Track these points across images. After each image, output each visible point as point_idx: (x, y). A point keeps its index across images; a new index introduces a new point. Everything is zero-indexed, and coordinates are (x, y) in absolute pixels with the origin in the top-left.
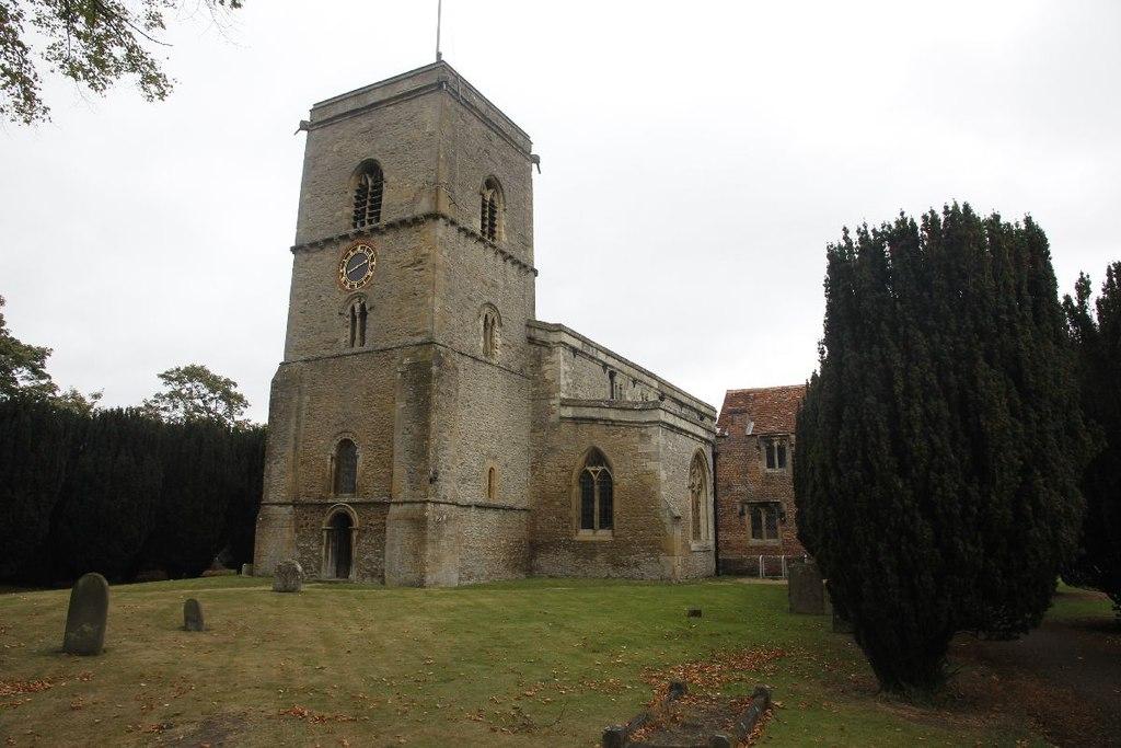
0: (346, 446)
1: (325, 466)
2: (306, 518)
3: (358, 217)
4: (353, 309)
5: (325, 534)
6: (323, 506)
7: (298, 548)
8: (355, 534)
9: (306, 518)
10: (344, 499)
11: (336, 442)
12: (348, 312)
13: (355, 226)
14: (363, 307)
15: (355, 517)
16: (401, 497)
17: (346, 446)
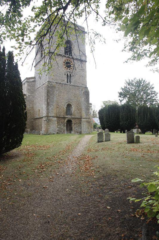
0: (69, 106)
1: (64, 109)
2: (59, 120)
3: (66, 52)
4: (68, 74)
5: (65, 124)
6: (64, 118)
7: (58, 127)
8: (73, 124)
9: (59, 120)
10: (69, 117)
11: (67, 104)
12: (67, 74)
13: (65, 54)
14: (70, 75)
15: (73, 121)
16: (84, 117)
17: (69, 106)
